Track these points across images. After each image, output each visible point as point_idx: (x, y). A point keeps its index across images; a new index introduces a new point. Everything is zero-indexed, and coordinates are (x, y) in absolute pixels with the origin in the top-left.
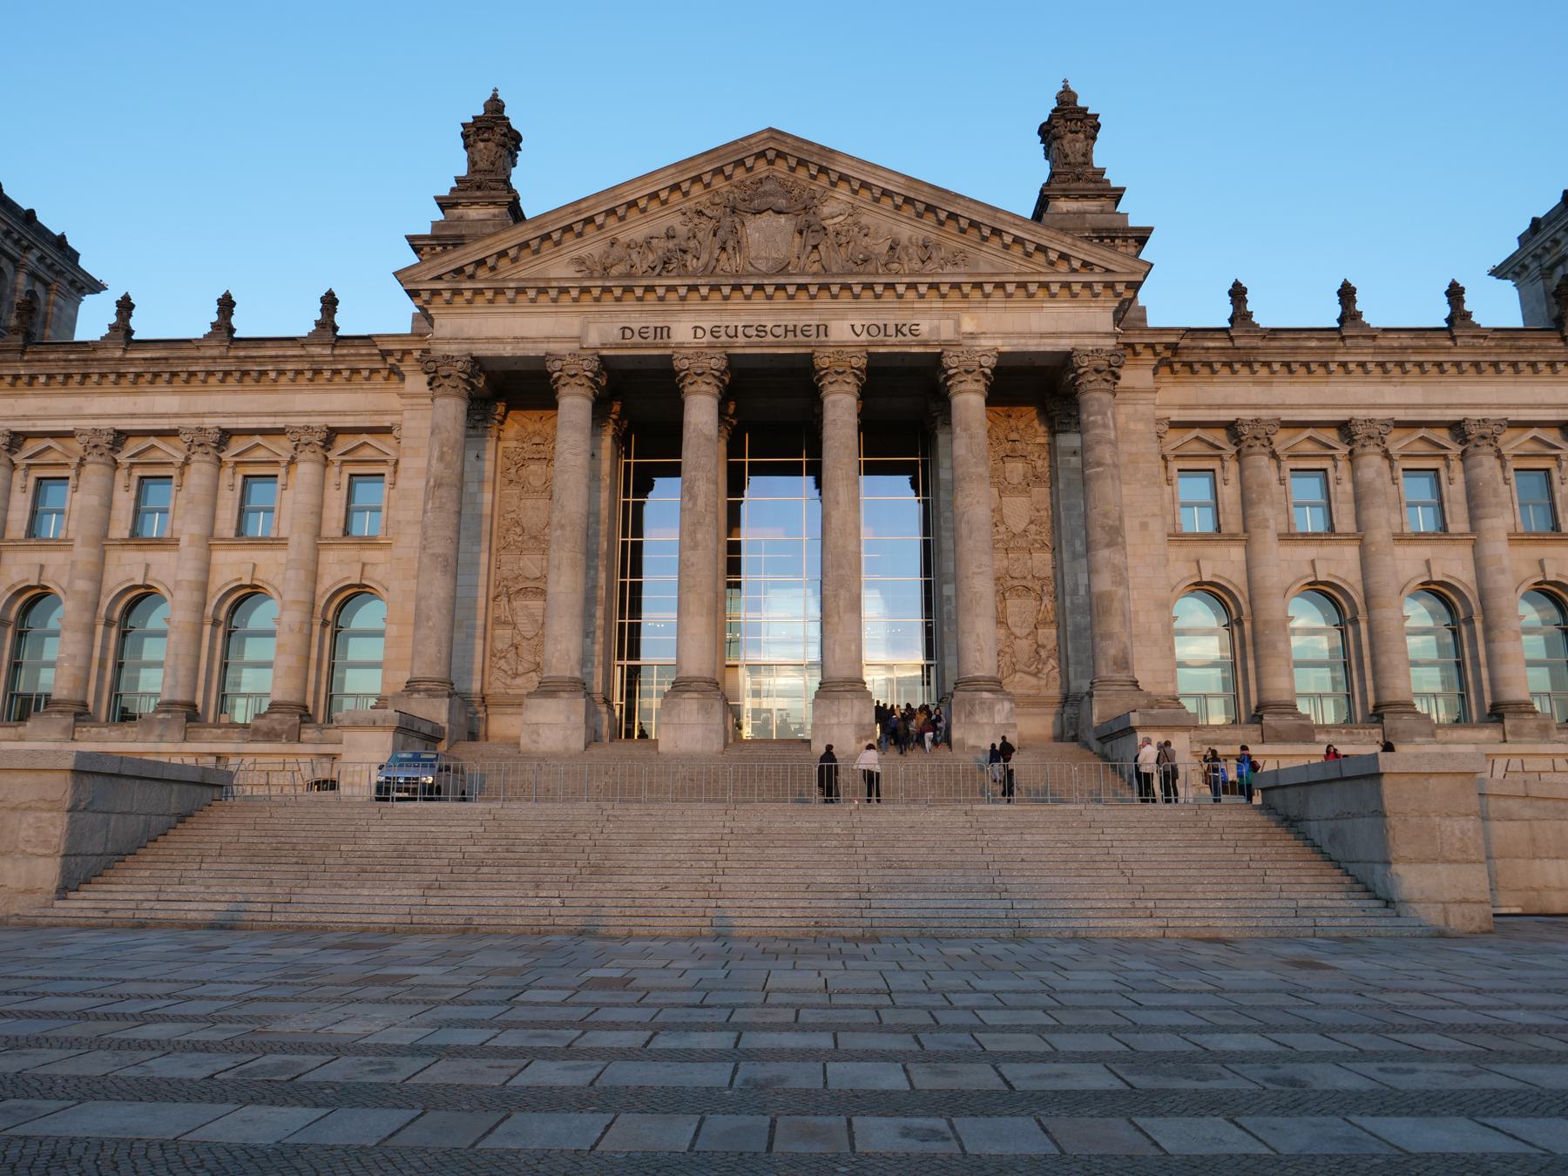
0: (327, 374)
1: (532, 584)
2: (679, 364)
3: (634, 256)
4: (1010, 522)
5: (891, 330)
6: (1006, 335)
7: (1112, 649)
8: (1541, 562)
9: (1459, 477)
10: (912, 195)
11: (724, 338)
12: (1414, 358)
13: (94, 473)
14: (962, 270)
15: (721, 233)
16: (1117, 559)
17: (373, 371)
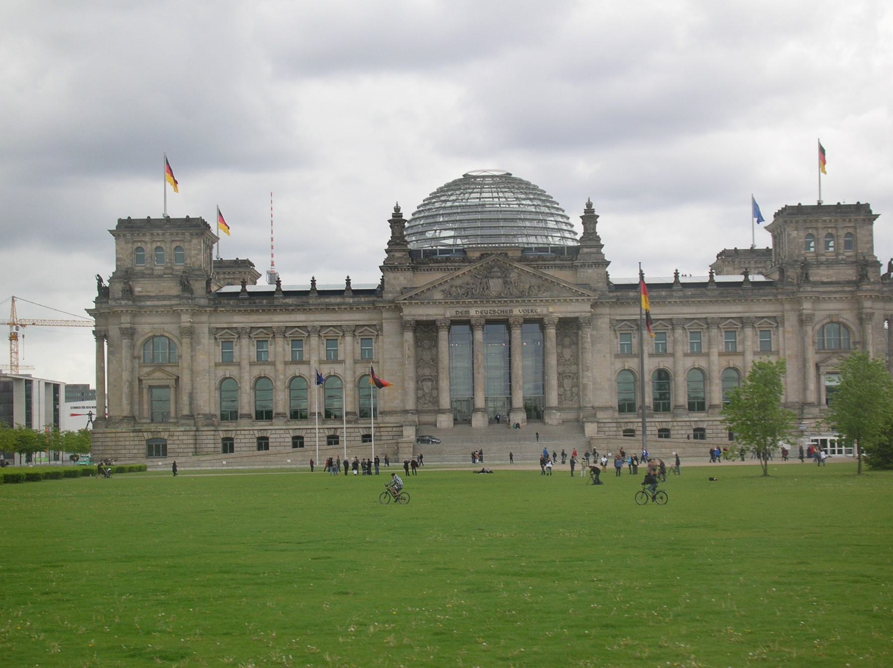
0: (354, 309)
1: (428, 377)
2: (473, 322)
3: (459, 290)
4: (565, 357)
5: (530, 311)
6: (560, 312)
7: (587, 399)
8: (729, 361)
9: (707, 334)
10: (535, 273)
12: (691, 300)
13: (280, 341)
14: (549, 293)
15: (482, 284)
16: (589, 374)
17: (369, 308)
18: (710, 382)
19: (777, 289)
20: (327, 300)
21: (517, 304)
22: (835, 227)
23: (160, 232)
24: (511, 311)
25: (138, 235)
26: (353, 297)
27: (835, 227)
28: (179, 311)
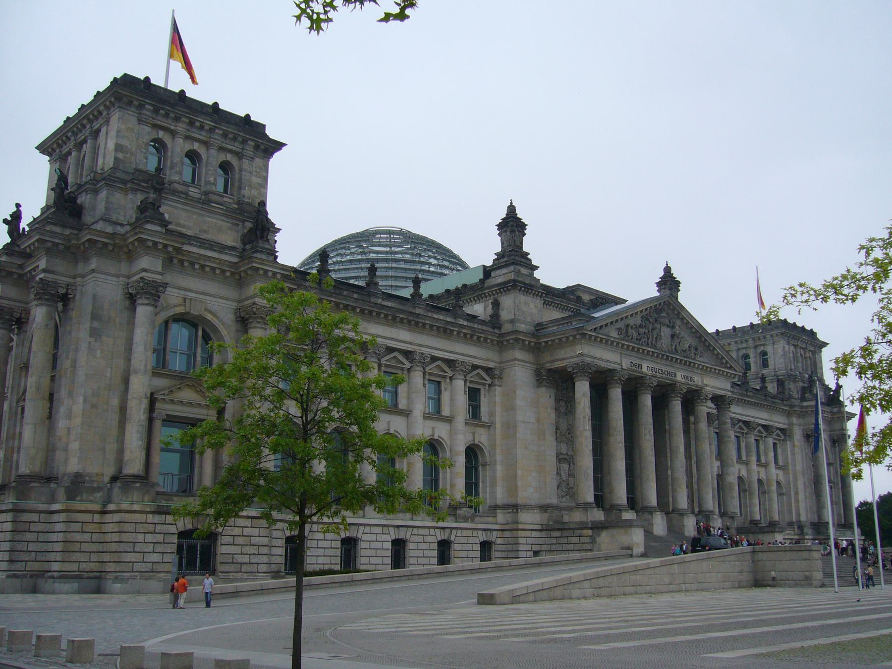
0: (475, 338)
6: (712, 387)
9: (744, 439)
11: (654, 373)
15: (657, 331)
17: (492, 340)
18: (751, 494)
19: (782, 401)
20: (435, 316)
21: (682, 366)
22: (803, 348)
23: (209, 123)
24: (675, 374)
25: (167, 116)
26: (468, 321)
27: (803, 348)
28: (261, 272)
